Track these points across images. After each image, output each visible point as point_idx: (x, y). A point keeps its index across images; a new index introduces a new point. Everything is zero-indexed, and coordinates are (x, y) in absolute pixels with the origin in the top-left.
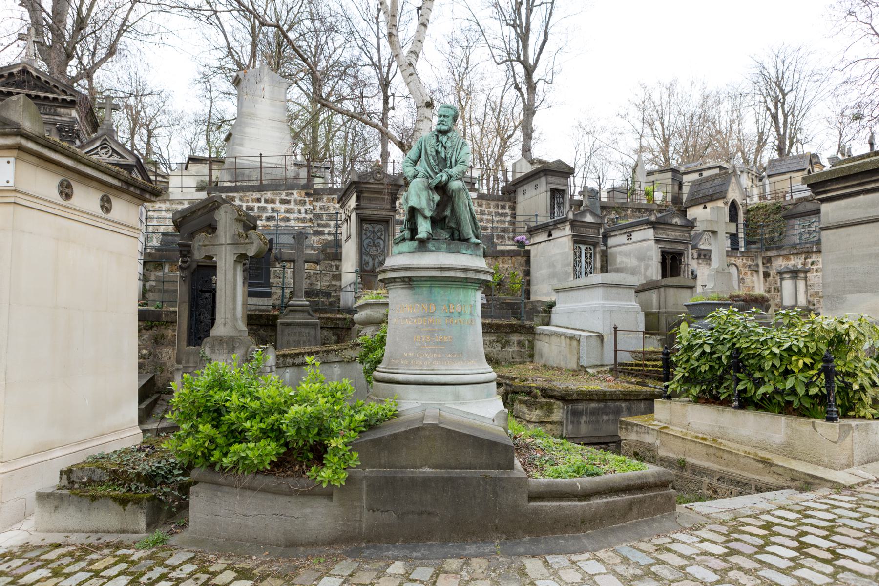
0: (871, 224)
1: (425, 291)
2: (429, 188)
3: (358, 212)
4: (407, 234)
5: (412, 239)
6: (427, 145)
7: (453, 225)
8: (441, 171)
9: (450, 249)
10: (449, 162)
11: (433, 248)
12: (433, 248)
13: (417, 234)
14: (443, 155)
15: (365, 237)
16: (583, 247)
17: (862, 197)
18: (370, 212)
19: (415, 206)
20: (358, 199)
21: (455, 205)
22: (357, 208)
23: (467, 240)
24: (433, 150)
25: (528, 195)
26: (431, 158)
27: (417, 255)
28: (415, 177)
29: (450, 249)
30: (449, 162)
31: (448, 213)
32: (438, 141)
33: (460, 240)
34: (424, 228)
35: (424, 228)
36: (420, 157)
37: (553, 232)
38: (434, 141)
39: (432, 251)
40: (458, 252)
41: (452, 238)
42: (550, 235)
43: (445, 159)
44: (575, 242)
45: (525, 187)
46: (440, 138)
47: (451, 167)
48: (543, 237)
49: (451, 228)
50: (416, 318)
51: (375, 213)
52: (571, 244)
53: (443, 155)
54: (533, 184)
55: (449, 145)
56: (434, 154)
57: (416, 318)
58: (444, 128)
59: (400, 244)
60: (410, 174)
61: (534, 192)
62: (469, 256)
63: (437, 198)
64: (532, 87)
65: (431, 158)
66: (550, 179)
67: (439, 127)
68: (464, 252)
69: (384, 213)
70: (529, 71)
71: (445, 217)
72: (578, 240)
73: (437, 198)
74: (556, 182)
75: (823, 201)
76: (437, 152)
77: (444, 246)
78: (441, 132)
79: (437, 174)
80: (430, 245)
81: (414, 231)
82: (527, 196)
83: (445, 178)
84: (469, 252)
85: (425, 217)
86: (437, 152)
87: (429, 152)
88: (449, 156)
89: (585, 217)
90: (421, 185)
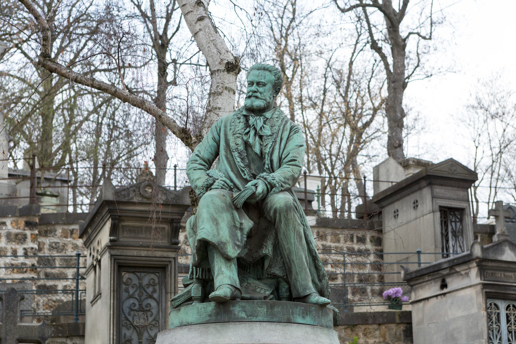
2: (233, 206)
3: (114, 252)
4: (195, 290)
5: (204, 298)
6: (230, 133)
7: (277, 271)
8: (254, 177)
9: (273, 315)
10: (267, 162)
11: (243, 315)
12: (243, 315)
13: (213, 289)
14: (257, 150)
15: (125, 295)
16: (502, 305)
18: (135, 253)
19: (209, 238)
20: (113, 231)
21: (281, 236)
22: (112, 245)
23: (304, 299)
24: (239, 141)
26: (236, 154)
27: (212, 327)
28: (208, 187)
29: (273, 315)
30: (267, 162)
31: (268, 250)
32: (247, 125)
33: (290, 298)
34: (225, 278)
35: (225, 278)
36: (217, 154)
37: (448, 280)
38: (242, 125)
39: (241, 321)
40: (289, 322)
41: (277, 295)
42: (444, 286)
43: (261, 157)
44: (488, 296)
45: (397, 205)
46: (252, 120)
47: (272, 170)
48: (431, 289)
49: (274, 276)
51: (143, 253)
52: (481, 299)
53: (257, 150)
54: (410, 200)
55: (267, 131)
56: (241, 148)
58: (258, 103)
59: (183, 309)
60: (200, 183)
61: (412, 214)
62: (308, 329)
63: (248, 224)
64: (399, 45)
65: (236, 154)
66: (439, 190)
67: (249, 102)
68: (300, 320)
69: (159, 254)
70: (393, 20)
71: (264, 258)
72: (493, 293)
73: (248, 224)
74: (449, 197)
76: (247, 145)
77: (263, 310)
78: (252, 110)
79: (247, 181)
80: (237, 310)
81: (207, 283)
82: (400, 220)
83: (261, 188)
84: (308, 320)
85: (228, 259)
86: (247, 145)
87: (232, 145)
88: (267, 150)
89: (503, 252)
90: (218, 202)
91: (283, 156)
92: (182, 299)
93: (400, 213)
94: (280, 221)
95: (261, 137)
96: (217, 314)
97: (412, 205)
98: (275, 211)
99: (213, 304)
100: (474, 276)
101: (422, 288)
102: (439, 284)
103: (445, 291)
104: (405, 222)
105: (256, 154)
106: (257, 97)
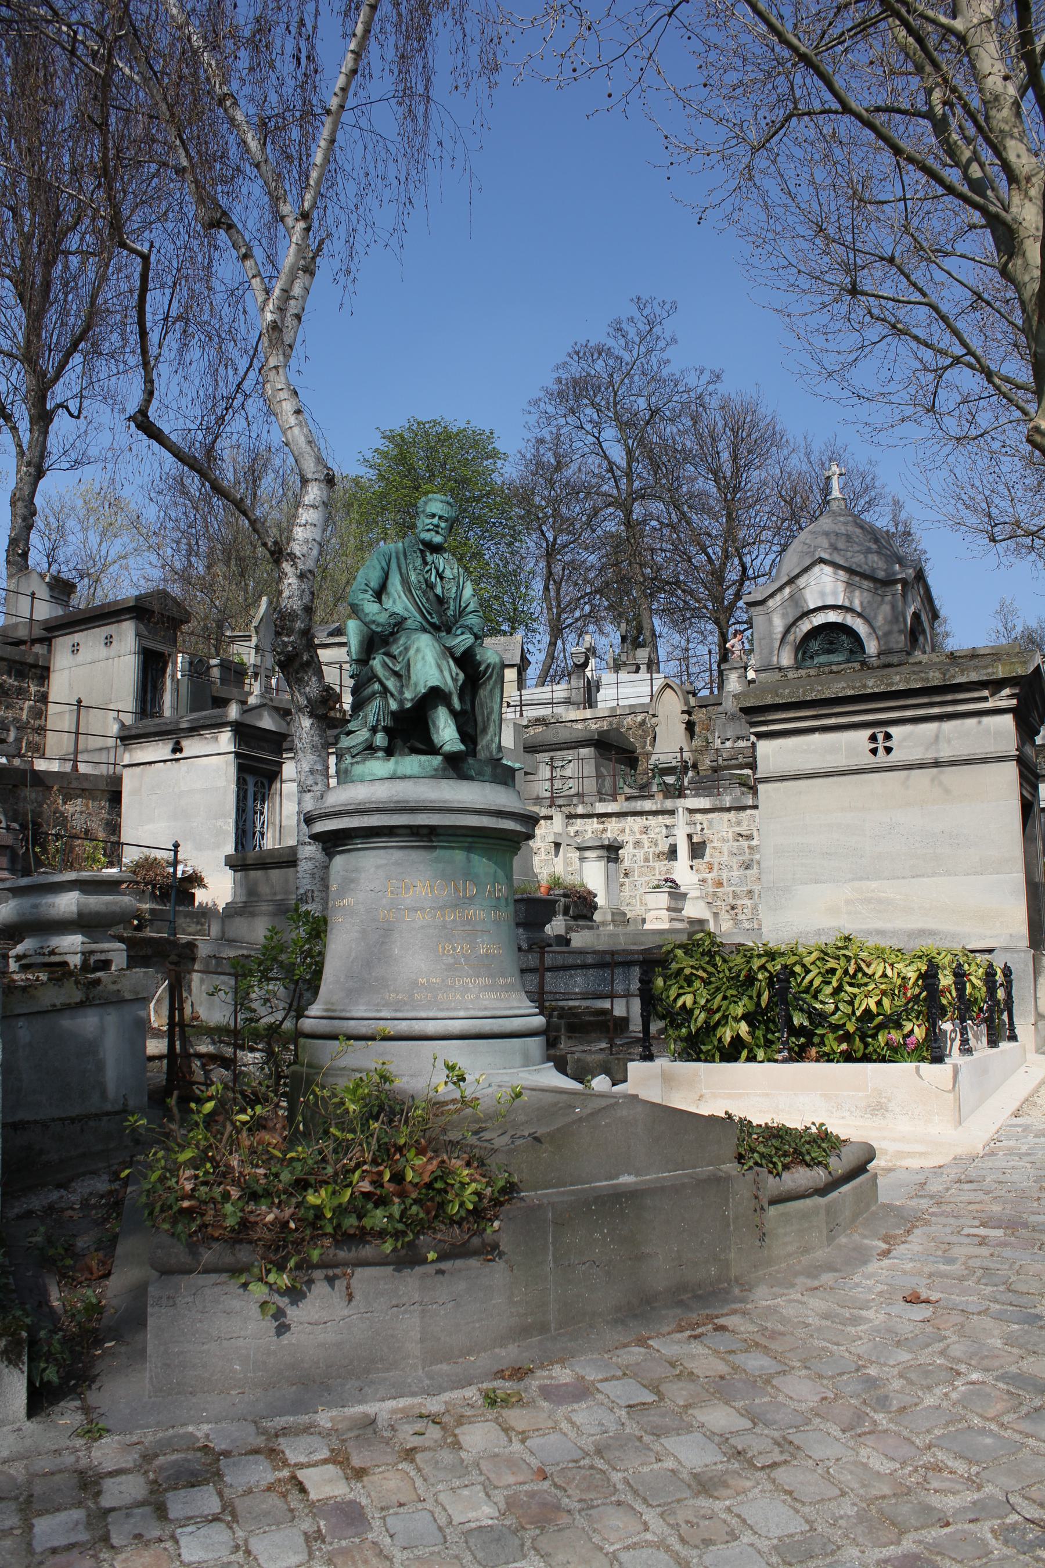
0: (821, 780)
1: (459, 856)
17: (817, 737)
24: (421, 579)
25: (84, 655)
32: (425, 563)
37: (185, 743)
38: (419, 561)
39: (470, 778)
45: (77, 637)
48: (161, 750)
50: (440, 908)
52: (232, 772)
53: (439, 590)
54: (102, 632)
57: (440, 908)
58: (438, 539)
61: (103, 652)
75: (760, 736)
82: (80, 657)
89: (260, 717)
91: (463, 605)
92: (361, 748)
93: (81, 648)
94: (490, 677)
95: (442, 578)
96: (444, 769)
97: (103, 641)
98: (488, 666)
99: (440, 758)
100: (225, 740)
101: (142, 749)
102: (170, 745)
103: (178, 755)
104: (89, 660)
105: (437, 596)
106: (437, 533)
